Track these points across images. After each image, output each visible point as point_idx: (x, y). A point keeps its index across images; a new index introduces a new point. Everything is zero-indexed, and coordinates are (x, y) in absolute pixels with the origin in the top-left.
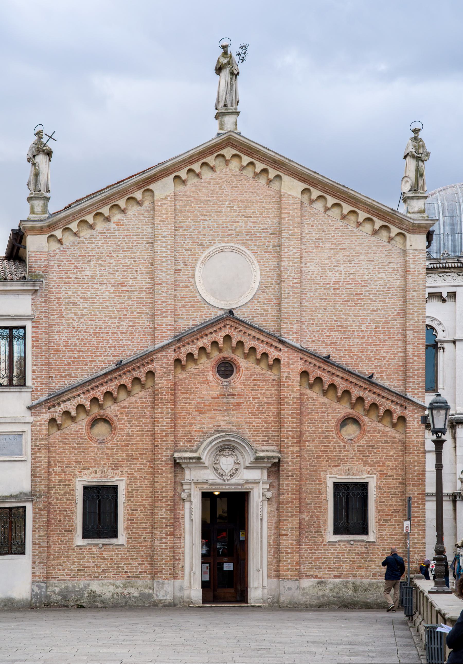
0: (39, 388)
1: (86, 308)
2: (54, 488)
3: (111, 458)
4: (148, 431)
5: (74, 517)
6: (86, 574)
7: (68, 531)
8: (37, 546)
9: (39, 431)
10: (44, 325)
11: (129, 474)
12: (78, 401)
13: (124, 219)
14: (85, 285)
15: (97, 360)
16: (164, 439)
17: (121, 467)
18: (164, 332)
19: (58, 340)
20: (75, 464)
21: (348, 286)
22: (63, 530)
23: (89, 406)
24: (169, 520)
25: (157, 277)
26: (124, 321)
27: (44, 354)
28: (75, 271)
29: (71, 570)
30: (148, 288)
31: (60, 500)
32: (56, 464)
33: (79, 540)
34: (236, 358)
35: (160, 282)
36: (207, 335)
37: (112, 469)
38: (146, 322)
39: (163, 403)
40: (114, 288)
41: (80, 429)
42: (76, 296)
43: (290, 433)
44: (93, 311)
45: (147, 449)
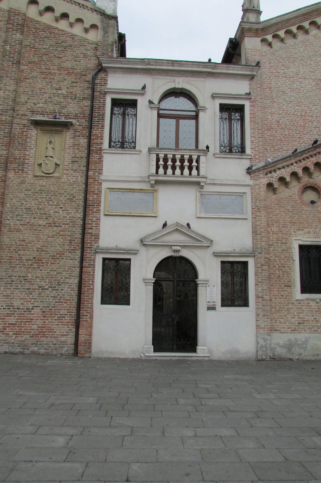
0: (257, 157)
1: (293, 96)
2: (273, 245)
5: (292, 273)
6: (306, 328)
7: (287, 286)
8: (261, 299)
10: (260, 105)
12: (292, 169)
14: (292, 79)
19: (271, 119)
20: (290, 225)
22: (283, 285)
23: (301, 173)
27: (260, 128)
28: (283, 68)
29: (292, 323)
31: (279, 257)
33: (298, 294)
40: (314, 83)
41: (293, 194)
42: (284, 87)
44: (299, 98)
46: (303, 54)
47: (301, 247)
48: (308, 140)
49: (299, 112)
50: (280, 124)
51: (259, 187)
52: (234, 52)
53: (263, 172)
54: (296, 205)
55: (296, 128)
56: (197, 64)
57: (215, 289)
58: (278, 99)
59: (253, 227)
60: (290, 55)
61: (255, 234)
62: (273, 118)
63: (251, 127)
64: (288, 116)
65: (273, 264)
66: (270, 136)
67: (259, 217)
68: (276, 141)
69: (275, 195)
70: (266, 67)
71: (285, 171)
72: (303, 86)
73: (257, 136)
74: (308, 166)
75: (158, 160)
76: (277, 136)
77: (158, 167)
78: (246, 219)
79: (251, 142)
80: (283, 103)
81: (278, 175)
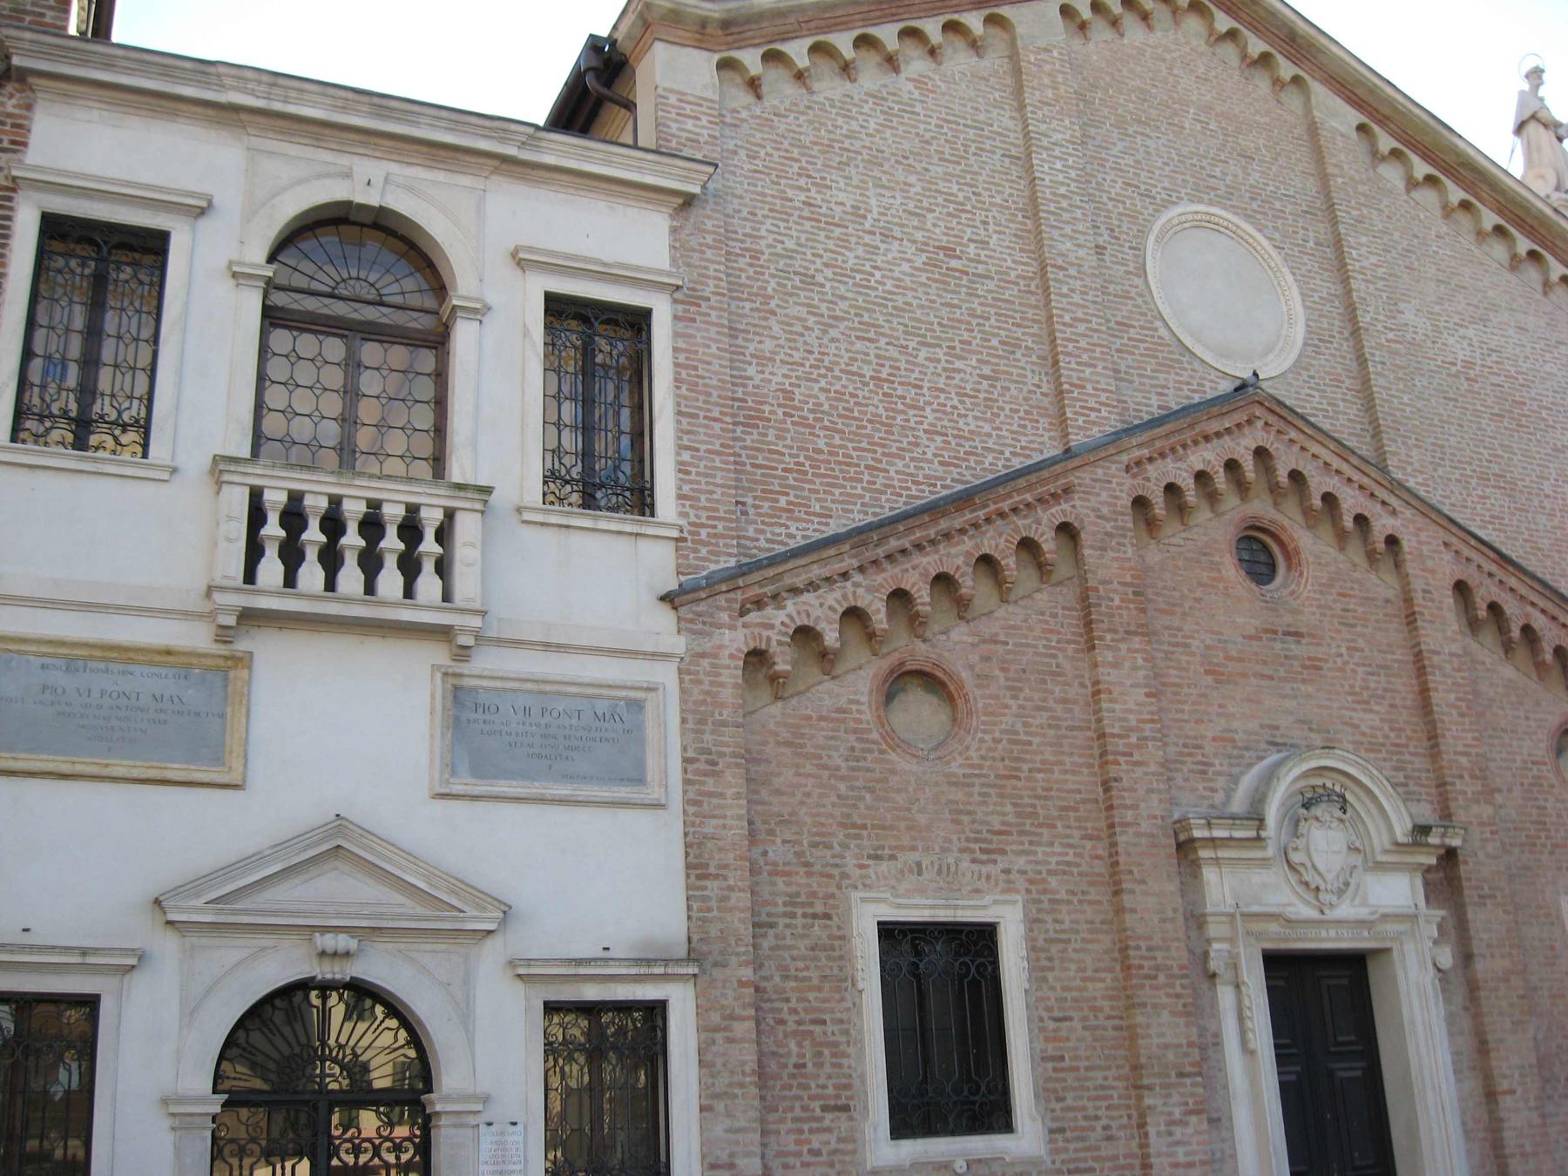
0: (704, 533)
1: (843, 298)
2: (772, 926)
3: (965, 819)
4: (1072, 728)
5: (851, 1050)
9: (708, 693)
11: (1031, 882)
12: (845, 596)
13: (937, 77)
14: (838, 231)
15: (892, 470)
16: (1136, 757)
17: (1003, 852)
18: (1092, 409)
19: (757, 382)
21: (1494, 379)
22: (816, 1105)
23: (882, 615)
24: (1186, 1055)
25: (1052, 247)
26: (965, 359)
27: (716, 414)
28: (802, 182)
30: (1024, 278)
31: (796, 979)
32: (771, 832)
34: (1286, 523)
35: (1060, 262)
36: (1207, 438)
37: (974, 861)
38: (1029, 374)
39: (1115, 631)
43: (1464, 760)
44: (868, 310)
45: (1079, 792)
46: (876, 140)
47: (887, 931)
48: (907, 481)
49: (869, 363)
50: (796, 403)
51: (713, 665)
52: (605, 91)
53: (727, 601)
54: (863, 750)
55: (858, 427)
56: (454, 116)
57: (515, 1137)
58: (787, 302)
59: (687, 845)
60: (832, 136)
61: (699, 877)
62: (767, 376)
63: (679, 404)
64: (825, 376)
65: (772, 1010)
66: (758, 450)
67: (715, 801)
68: (779, 472)
69: (779, 704)
70: (738, 171)
71: (817, 603)
72: (879, 264)
73: (703, 447)
74: (906, 586)
75: (257, 516)
76: (783, 454)
77: (254, 552)
78: (658, 806)
79: (680, 471)
80: (806, 320)
81: (790, 616)
